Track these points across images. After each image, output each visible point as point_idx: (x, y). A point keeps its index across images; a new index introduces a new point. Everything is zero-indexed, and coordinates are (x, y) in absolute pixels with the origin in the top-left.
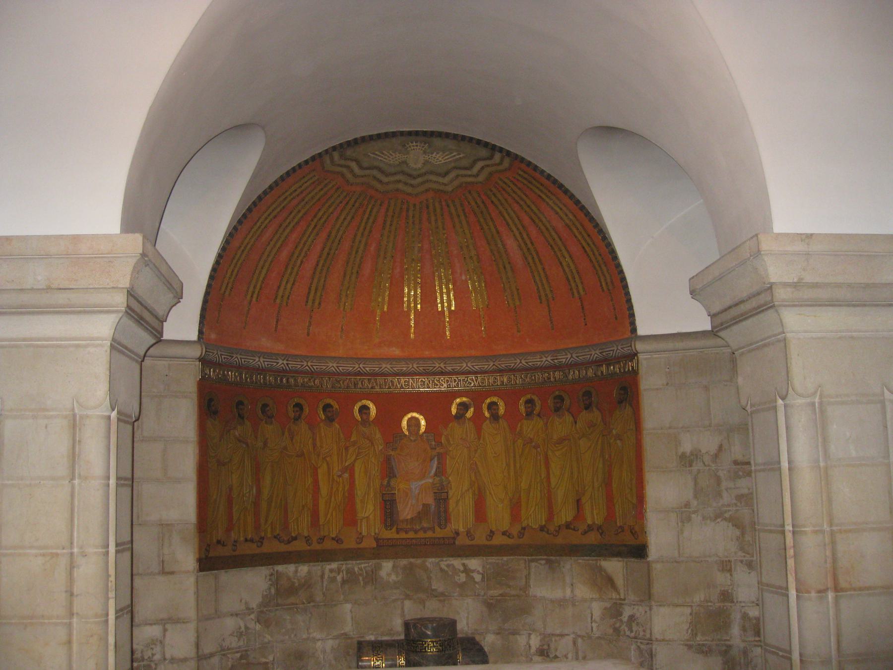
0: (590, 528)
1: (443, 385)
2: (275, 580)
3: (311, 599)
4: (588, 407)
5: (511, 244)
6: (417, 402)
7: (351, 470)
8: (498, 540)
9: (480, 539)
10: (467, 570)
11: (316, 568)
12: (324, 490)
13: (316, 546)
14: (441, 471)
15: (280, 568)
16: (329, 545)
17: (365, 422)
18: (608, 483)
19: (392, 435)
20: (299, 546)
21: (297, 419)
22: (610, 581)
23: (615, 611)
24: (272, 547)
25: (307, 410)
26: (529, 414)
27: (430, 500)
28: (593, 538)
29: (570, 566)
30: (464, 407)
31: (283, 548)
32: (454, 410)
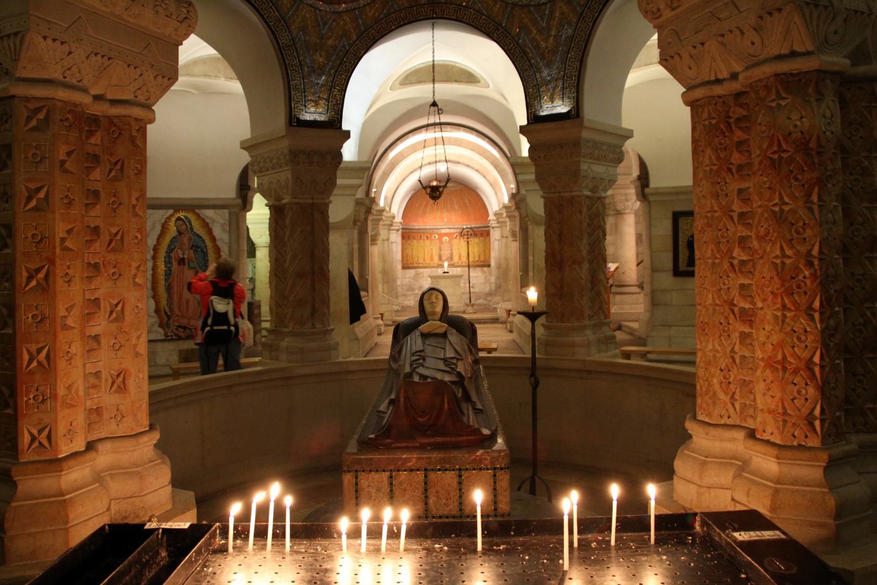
0: (481, 262)
1: (452, 231)
2: (416, 272)
3: (423, 276)
4: (482, 236)
5: (467, 201)
6: (446, 234)
7: (432, 249)
8: (464, 264)
9: (460, 264)
10: (457, 270)
11: (425, 270)
12: (426, 253)
13: (424, 265)
14: (451, 250)
15: (417, 270)
16: (427, 265)
17: (435, 239)
18: (485, 252)
19: (441, 242)
20: (421, 265)
21: (420, 239)
22: (485, 272)
23: (485, 278)
24: (415, 265)
25: (422, 237)
27: (449, 256)
28: (482, 263)
29: (478, 269)
30: (457, 236)
31: (417, 265)
32: (455, 236)
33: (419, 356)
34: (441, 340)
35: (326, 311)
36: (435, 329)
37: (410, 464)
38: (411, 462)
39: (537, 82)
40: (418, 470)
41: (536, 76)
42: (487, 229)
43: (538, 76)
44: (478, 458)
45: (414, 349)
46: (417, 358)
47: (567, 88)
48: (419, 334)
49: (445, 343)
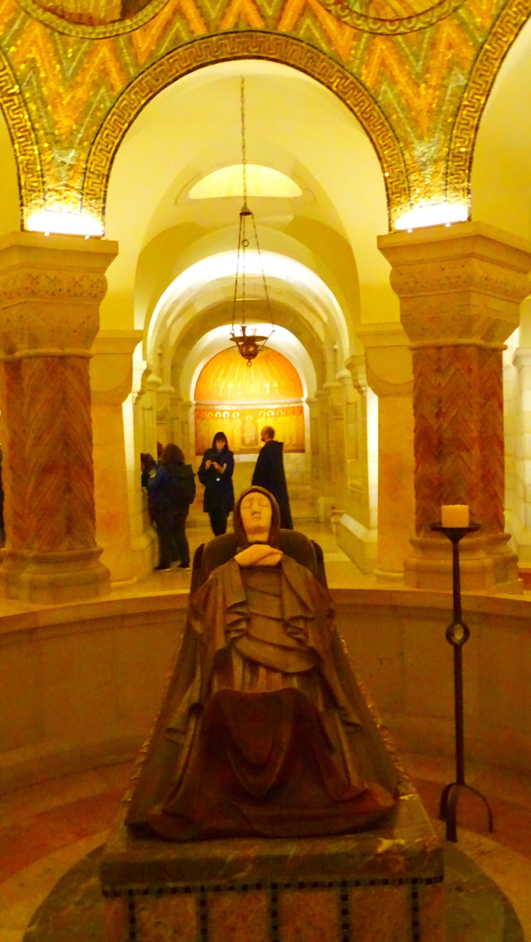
0: (294, 445)
26: (279, 416)
28: (294, 448)
30: (263, 414)
32: (260, 414)
33: (239, 613)
34: (273, 579)
35: (90, 523)
36: (261, 559)
37: (240, 875)
38: (242, 871)
39: (405, 165)
40: (259, 887)
41: (403, 155)
42: (300, 405)
43: (407, 156)
44: (379, 860)
45: (233, 600)
46: (236, 617)
47: (452, 174)
48: (237, 568)
49: (281, 584)
